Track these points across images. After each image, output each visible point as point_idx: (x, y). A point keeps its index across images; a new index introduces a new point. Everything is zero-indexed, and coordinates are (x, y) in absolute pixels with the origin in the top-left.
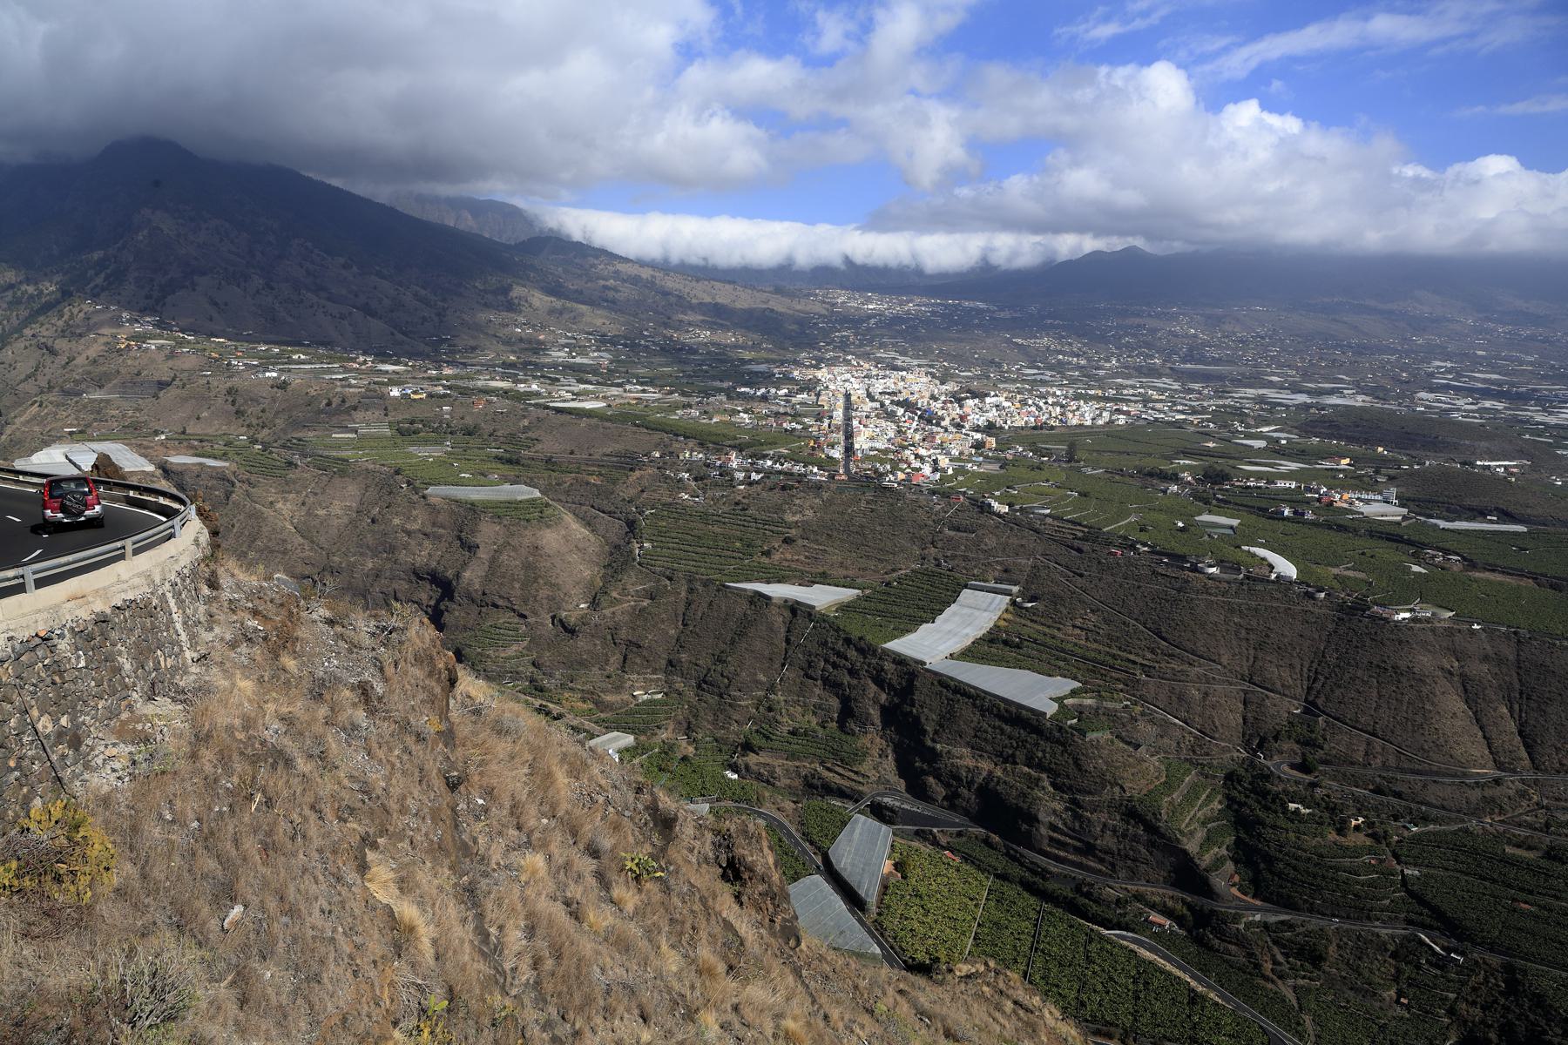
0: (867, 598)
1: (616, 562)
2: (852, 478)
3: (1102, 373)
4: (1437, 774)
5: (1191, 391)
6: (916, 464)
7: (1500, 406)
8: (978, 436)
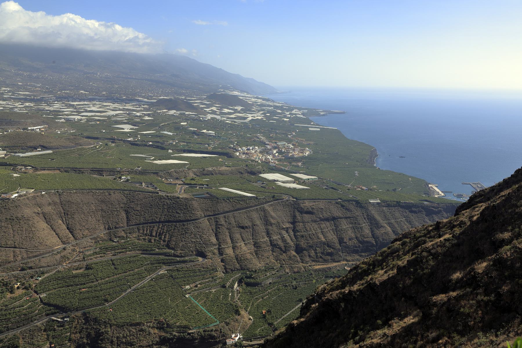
4: (43, 254)
7: (32, 105)
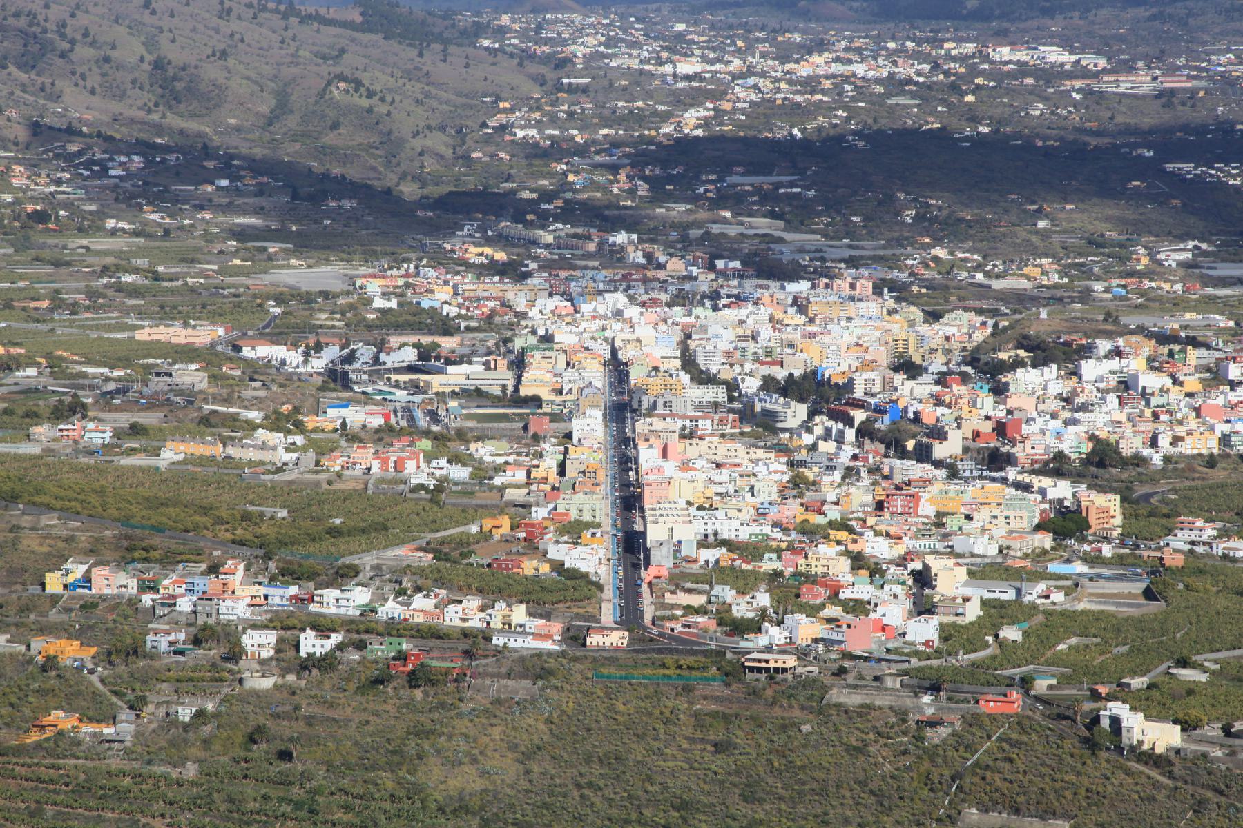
6: (862, 589)
8: (1062, 490)
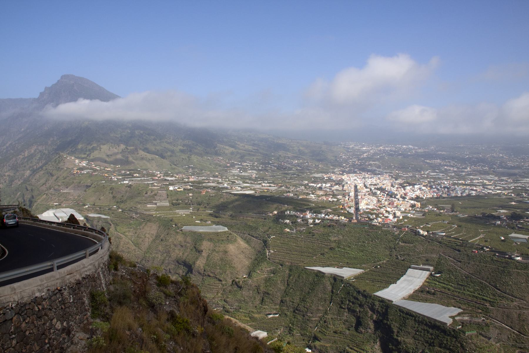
0: (365, 273)
1: (259, 259)
2: (359, 221)
3: (464, 174)
5: (502, 180)
6: (386, 215)
8: (412, 202)
